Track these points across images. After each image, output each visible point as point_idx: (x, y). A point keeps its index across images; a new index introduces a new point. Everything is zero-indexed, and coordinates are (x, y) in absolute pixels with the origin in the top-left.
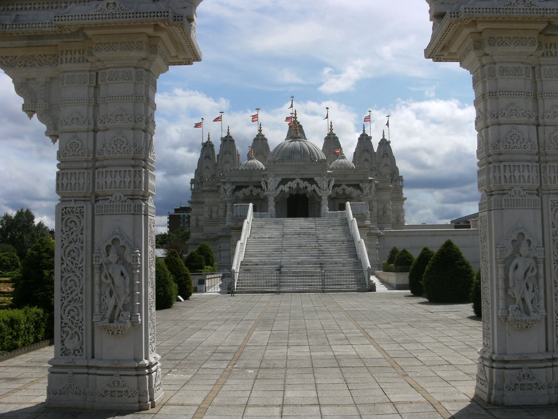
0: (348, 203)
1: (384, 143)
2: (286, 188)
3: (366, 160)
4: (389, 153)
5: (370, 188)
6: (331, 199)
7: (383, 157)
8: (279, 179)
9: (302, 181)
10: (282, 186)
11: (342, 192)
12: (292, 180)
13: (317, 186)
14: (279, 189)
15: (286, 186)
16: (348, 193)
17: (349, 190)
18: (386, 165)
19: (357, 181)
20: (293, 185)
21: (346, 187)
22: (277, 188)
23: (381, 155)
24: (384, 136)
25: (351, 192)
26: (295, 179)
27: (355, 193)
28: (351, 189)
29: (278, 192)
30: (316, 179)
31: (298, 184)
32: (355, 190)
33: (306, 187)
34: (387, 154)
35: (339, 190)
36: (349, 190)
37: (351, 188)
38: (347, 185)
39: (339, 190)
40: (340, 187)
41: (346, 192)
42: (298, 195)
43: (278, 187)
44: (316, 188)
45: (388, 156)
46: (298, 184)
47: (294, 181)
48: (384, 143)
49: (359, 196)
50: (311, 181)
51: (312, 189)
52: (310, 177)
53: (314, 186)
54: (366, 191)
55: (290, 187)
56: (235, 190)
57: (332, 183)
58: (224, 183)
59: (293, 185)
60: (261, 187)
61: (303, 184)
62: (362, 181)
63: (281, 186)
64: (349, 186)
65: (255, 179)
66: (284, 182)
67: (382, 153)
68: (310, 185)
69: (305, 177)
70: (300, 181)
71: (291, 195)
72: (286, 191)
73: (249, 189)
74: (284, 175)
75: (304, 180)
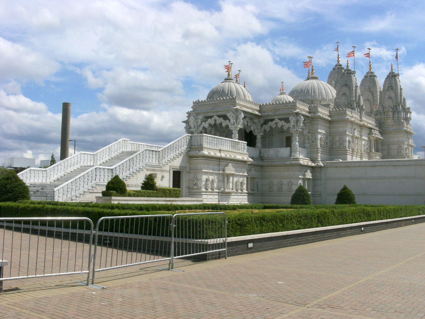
4: (394, 85)
6: (240, 131)
7: (388, 90)
8: (201, 117)
9: (218, 118)
11: (275, 126)
12: (211, 117)
16: (279, 126)
17: (281, 123)
18: (390, 98)
19: (285, 114)
20: (211, 121)
21: (278, 121)
23: (386, 88)
25: (282, 126)
26: (213, 116)
28: (283, 123)
30: (228, 115)
31: (215, 120)
32: (285, 123)
34: (391, 86)
37: (283, 121)
38: (279, 119)
40: (273, 122)
41: (278, 125)
44: (228, 123)
45: (392, 89)
46: (215, 120)
47: (213, 118)
50: (225, 117)
52: (223, 113)
53: (227, 121)
59: (211, 121)
61: (220, 120)
62: (289, 114)
63: (204, 123)
64: (281, 119)
68: (224, 121)
69: (220, 113)
70: (217, 118)
74: (204, 113)
75: (220, 116)
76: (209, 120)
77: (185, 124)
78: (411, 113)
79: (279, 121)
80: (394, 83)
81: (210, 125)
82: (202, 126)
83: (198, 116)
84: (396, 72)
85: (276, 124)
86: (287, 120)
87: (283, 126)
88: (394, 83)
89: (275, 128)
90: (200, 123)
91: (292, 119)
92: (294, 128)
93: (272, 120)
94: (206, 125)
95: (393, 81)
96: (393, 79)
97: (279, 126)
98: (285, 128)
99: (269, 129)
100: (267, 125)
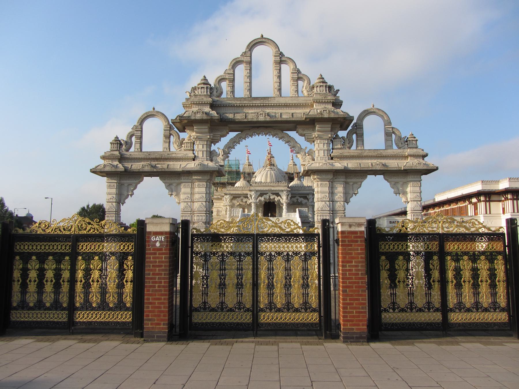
0: (297, 209)
2: (262, 199)
8: (259, 193)
10: (260, 198)
12: (266, 194)
17: (300, 200)
20: (267, 197)
21: (298, 198)
25: (301, 202)
27: (304, 201)
28: (302, 199)
35: (295, 200)
39: (295, 200)
42: (269, 202)
46: (270, 196)
49: (306, 203)
56: (232, 199)
57: (290, 196)
58: (226, 194)
59: (267, 197)
60: (248, 198)
62: (308, 194)
64: (300, 197)
65: (245, 192)
66: (261, 195)
70: (271, 195)
71: (266, 202)
73: (241, 198)
75: (273, 194)
82: (259, 199)
85: (297, 199)
87: (301, 202)
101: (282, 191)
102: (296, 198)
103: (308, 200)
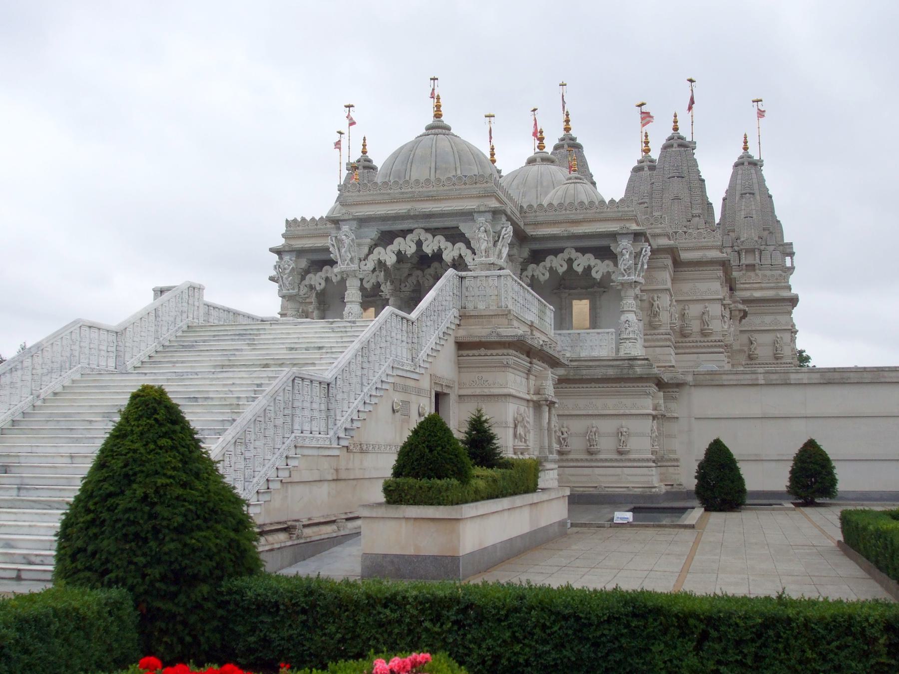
1: (748, 167)
2: (388, 256)
3: (677, 198)
5: (637, 255)
8: (372, 233)
9: (429, 236)
12: (404, 233)
13: (468, 245)
14: (371, 256)
15: (389, 248)
16: (580, 270)
17: (582, 262)
21: (574, 254)
22: (366, 258)
24: (746, 149)
25: (588, 269)
26: (411, 231)
27: (600, 269)
29: (370, 264)
30: (464, 228)
31: (419, 244)
32: (598, 261)
33: (440, 249)
36: (582, 262)
37: (590, 256)
38: (578, 250)
43: (370, 252)
46: (419, 244)
47: (409, 237)
48: (748, 167)
51: (456, 254)
52: (449, 223)
54: (626, 260)
55: (399, 252)
59: (408, 246)
62: (613, 236)
63: (379, 249)
64: (583, 251)
66: (386, 238)
67: (738, 187)
68: (449, 244)
70: (424, 236)
72: (389, 263)
74: (384, 219)
75: (434, 232)
76: (399, 240)
77: (276, 257)
78: (792, 254)
79: (579, 254)
80: (755, 181)
81: (399, 254)
82: (374, 257)
83: (360, 227)
84: (756, 157)
85: (570, 261)
86: (605, 253)
87: (588, 269)
88: (755, 181)
89: (564, 273)
90: (366, 250)
91: (625, 246)
92: (629, 275)
93: (556, 252)
94: (388, 256)
95: (754, 176)
96: (753, 171)
97: (580, 270)
98: (597, 275)
99: (547, 275)
100: (542, 264)
101: (469, 215)
102: (565, 255)
103: (616, 265)
